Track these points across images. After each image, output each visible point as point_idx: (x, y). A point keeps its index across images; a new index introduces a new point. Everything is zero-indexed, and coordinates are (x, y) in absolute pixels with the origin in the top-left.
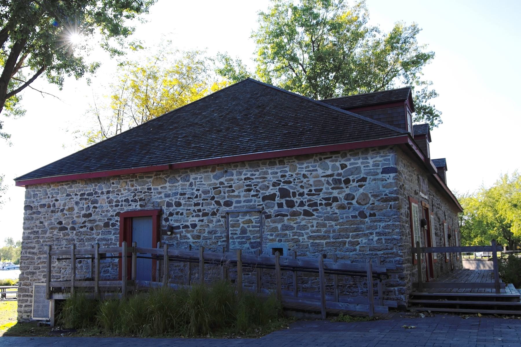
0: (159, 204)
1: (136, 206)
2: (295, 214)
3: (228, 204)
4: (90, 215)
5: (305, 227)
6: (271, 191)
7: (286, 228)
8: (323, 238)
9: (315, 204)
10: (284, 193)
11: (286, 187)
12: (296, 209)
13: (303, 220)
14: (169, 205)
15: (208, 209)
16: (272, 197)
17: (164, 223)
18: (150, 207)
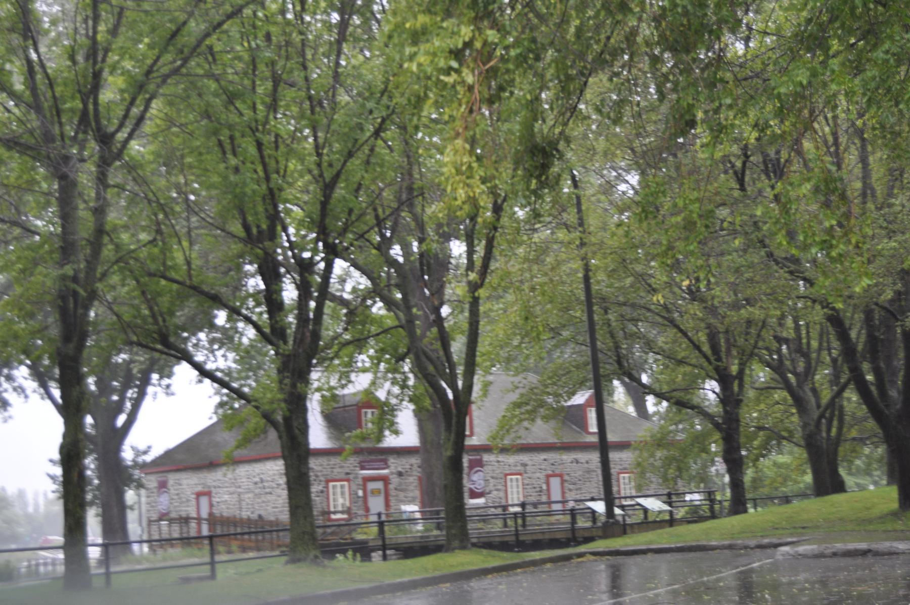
0: (209, 487)
1: (199, 489)
2: (267, 493)
3: (240, 487)
4: (178, 494)
5: (269, 501)
6: (257, 479)
7: (263, 502)
8: (276, 507)
9: (273, 488)
10: (262, 481)
11: (262, 476)
12: (268, 490)
13: (269, 497)
14: (215, 487)
15: (232, 489)
16: (256, 483)
17: (214, 499)
18: (206, 490)
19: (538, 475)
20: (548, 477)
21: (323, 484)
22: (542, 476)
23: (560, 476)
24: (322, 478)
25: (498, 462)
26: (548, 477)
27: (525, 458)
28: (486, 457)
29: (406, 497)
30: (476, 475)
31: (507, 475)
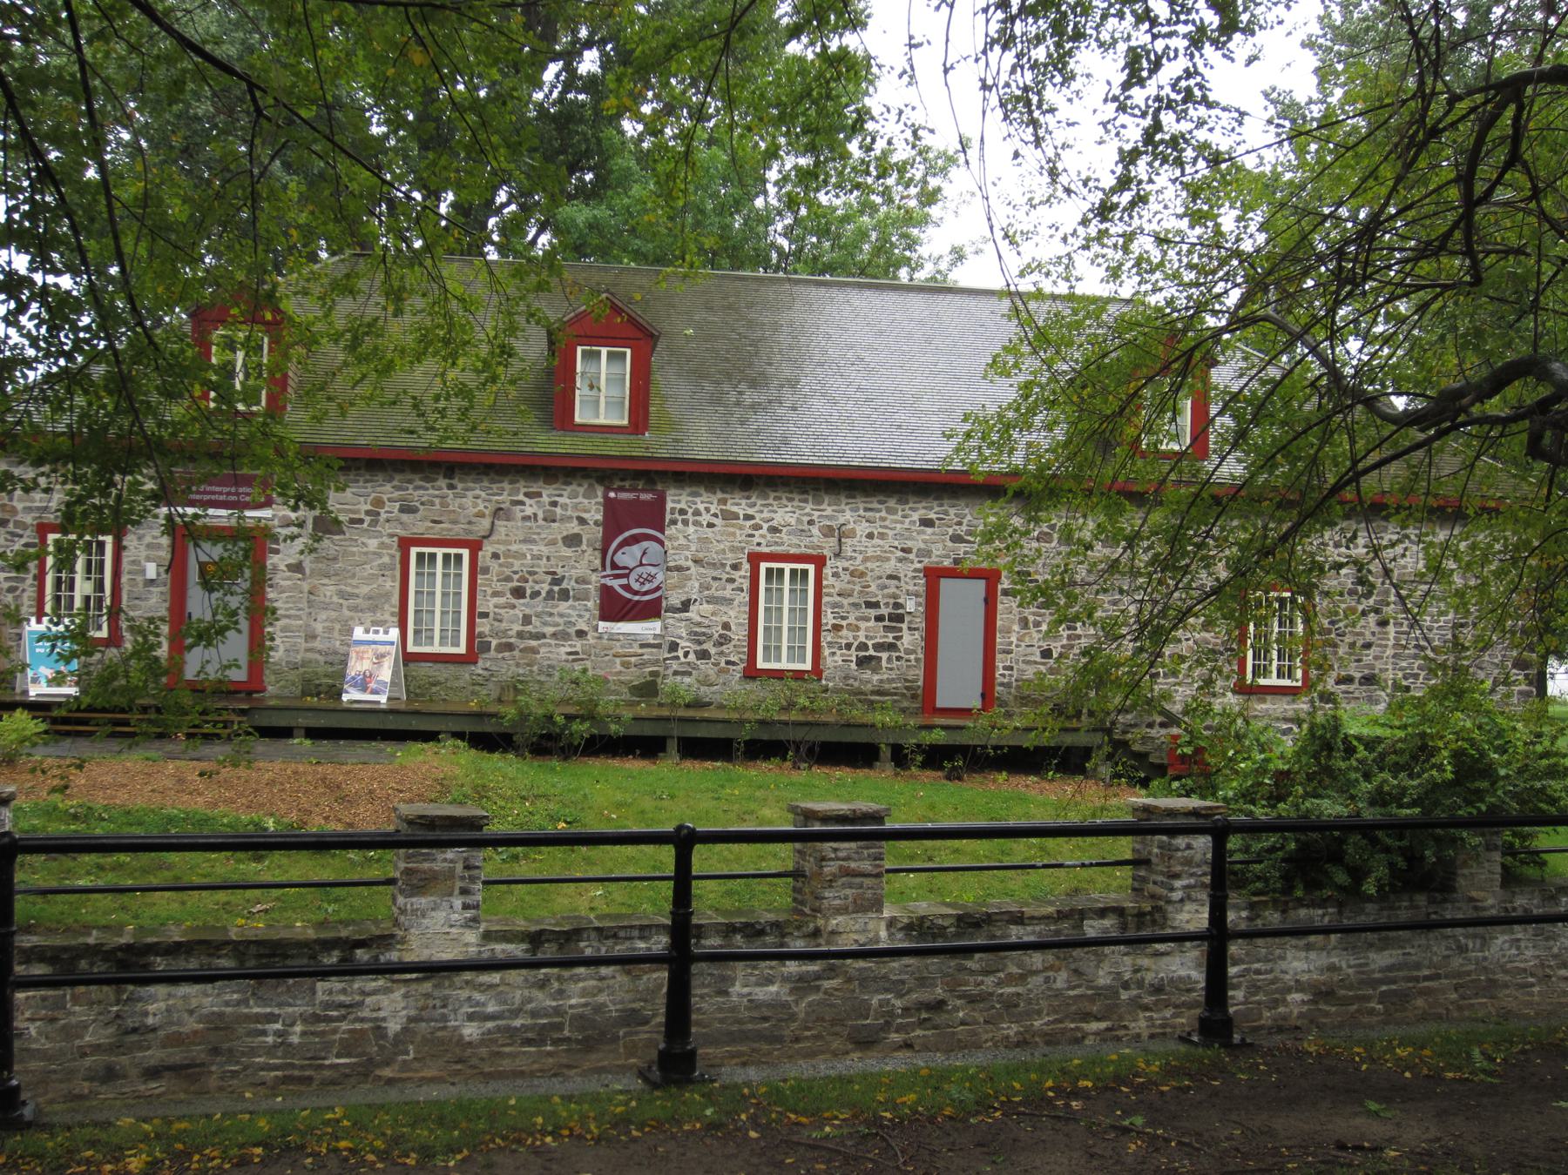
19: (891, 566)
20: (934, 576)
21: (29, 536)
22: (906, 571)
23: (990, 578)
24: (29, 519)
25: (729, 516)
26: (934, 576)
27: (847, 513)
28: (676, 500)
29: (342, 595)
30: (636, 550)
31: (755, 559)
